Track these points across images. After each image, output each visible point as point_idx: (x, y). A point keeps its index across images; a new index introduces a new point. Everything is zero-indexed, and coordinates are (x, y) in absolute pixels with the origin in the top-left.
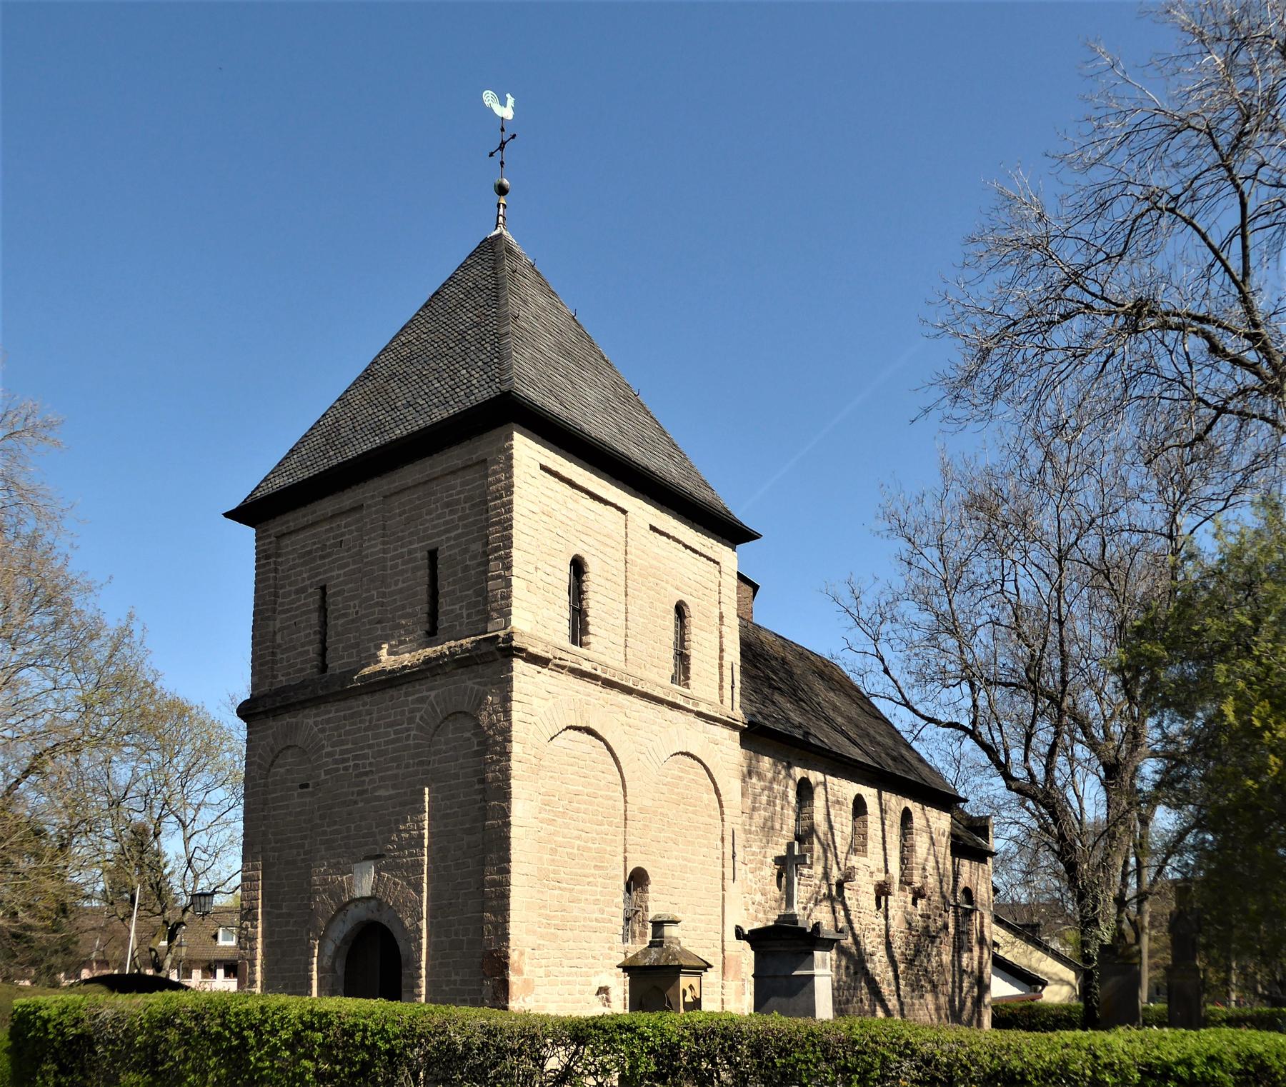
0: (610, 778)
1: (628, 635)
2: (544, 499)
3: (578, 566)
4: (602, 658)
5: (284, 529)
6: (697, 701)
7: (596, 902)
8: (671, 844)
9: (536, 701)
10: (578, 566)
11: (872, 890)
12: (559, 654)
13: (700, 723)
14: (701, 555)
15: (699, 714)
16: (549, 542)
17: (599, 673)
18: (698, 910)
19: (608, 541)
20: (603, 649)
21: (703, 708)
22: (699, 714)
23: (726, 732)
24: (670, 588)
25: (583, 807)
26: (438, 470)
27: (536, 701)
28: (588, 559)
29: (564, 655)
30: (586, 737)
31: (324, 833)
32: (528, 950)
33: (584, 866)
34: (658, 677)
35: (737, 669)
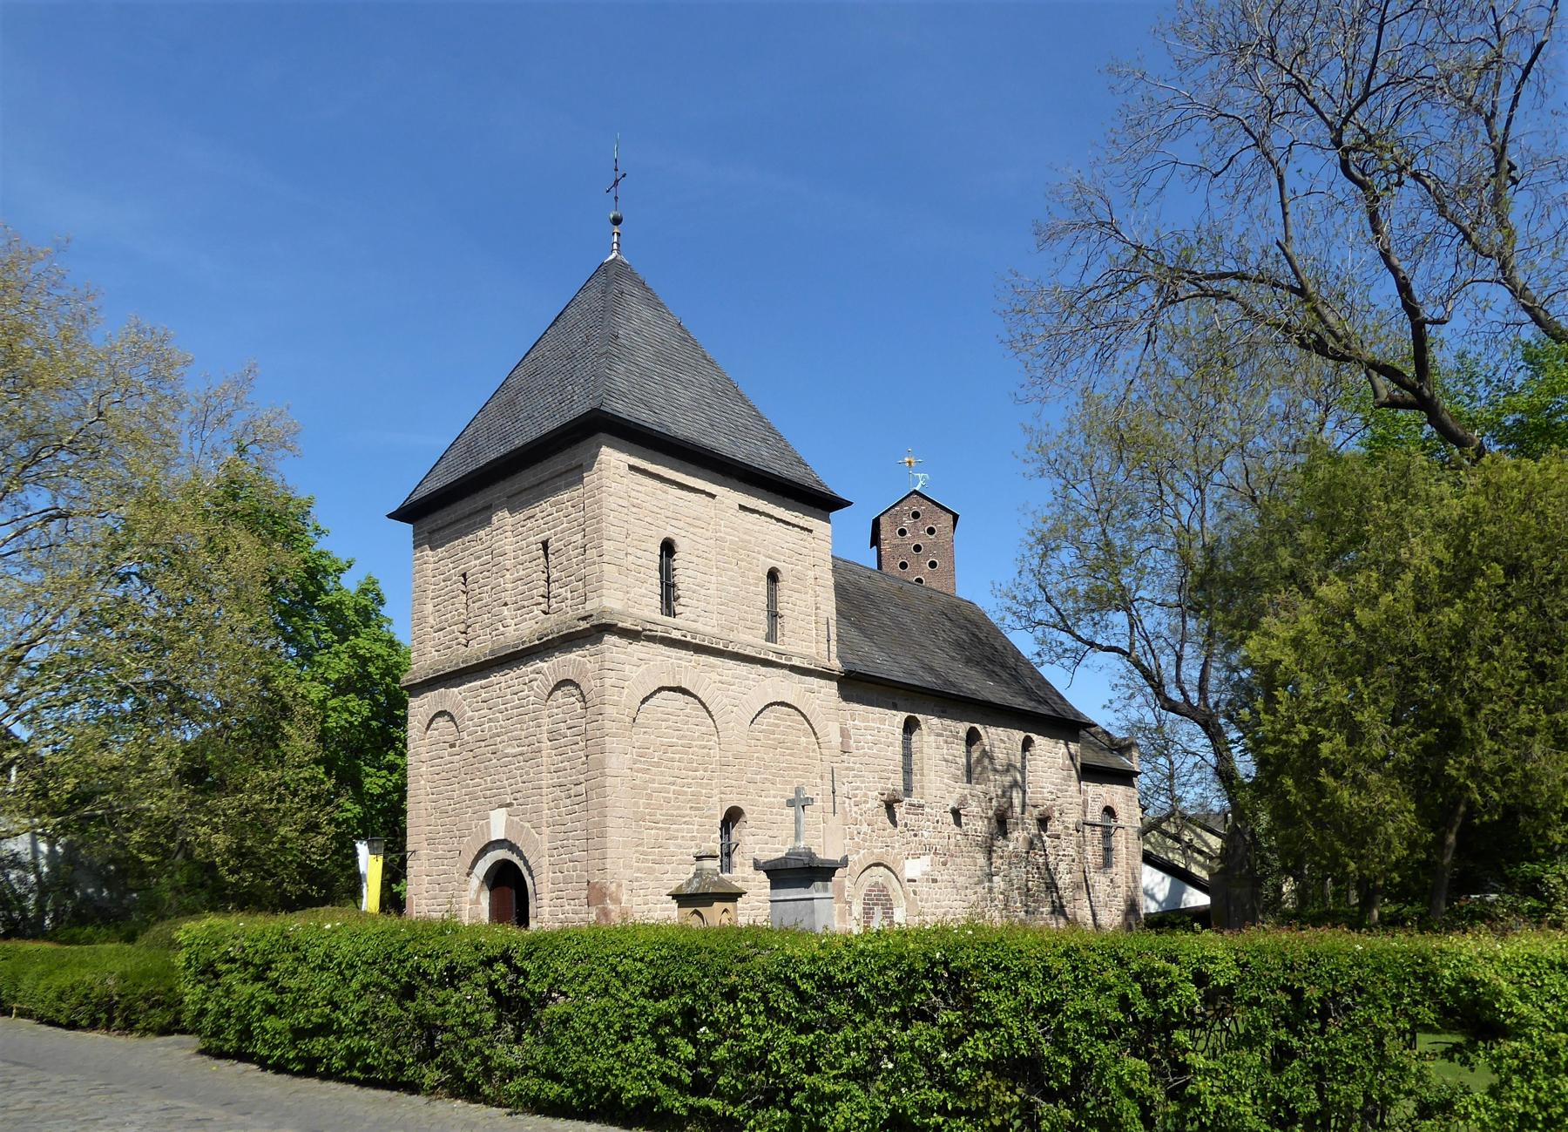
1: (716, 601)
2: (633, 494)
3: (668, 548)
4: (694, 626)
6: (790, 656)
7: (693, 839)
8: (768, 785)
9: (627, 667)
10: (668, 548)
12: (649, 626)
15: (793, 669)
16: (637, 529)
17: (689, 639)
21: (796, 662)
22: (793, 669)
23: (823, 682)
27: (627, 667)
28: (678, 540)
31: (468, 786)
32: (625, 882)
33: (679, 808)
35: (833, 623)
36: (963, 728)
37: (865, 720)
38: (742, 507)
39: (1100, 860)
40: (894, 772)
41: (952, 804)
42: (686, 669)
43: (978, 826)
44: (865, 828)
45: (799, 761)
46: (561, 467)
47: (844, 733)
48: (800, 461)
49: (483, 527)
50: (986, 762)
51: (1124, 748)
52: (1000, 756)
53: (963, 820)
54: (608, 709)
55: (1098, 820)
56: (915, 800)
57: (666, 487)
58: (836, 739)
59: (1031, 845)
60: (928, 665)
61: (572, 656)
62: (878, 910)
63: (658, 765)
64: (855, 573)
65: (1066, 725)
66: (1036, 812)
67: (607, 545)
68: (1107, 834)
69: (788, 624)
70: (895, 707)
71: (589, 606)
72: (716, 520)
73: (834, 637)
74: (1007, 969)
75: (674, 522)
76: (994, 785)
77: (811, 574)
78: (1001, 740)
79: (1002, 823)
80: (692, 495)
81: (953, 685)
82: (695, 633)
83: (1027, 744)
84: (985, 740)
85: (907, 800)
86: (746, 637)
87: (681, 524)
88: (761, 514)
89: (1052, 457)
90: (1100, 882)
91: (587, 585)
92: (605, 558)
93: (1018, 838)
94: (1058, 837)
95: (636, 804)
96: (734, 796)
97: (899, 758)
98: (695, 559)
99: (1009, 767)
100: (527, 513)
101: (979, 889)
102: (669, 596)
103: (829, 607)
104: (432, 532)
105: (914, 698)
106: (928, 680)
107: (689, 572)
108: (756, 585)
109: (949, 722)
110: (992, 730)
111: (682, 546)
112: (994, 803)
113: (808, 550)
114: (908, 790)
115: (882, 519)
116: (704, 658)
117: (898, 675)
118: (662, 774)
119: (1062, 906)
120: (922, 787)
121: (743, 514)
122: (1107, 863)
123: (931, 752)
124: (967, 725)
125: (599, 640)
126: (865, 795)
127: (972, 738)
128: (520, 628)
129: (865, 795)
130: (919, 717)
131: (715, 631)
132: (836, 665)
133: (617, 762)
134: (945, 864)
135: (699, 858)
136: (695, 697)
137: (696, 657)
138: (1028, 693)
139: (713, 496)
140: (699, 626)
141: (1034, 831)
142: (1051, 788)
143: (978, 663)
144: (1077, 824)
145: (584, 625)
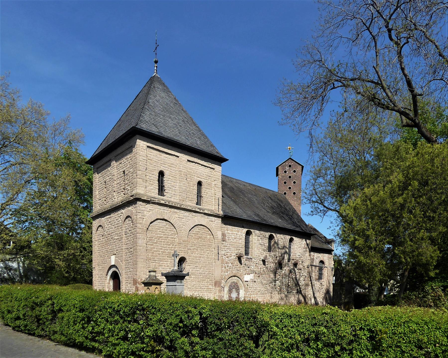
3: (161, 174)
4: (170, 199)
7: (168, 266)
9: (145, 212)
10: (161, 174)
14: (208, 167)
15: (205, 214)
16: (150, 167)
17: (167, 203)
18: (205, 268)
19: (172, 165)
21: (206, 212)
22: (205, 214)
23: (216, 218)
24: (196, 177)
25: (163, 241)
26: (124, 149)
27: (145, 212)
28: (165, 171)
29: (155, 199)
35: (220, 199)
36: (268, 234)
37: (232, 231)
38: (188, 161)
39: (317, 277)
40: (242, 248)
41: (262, 258)
43: (271, 265)
44: (230, 265)
45: (206, 243)
46: (127, 147)
47: (223, 235)
48: (212, 146)
49: (109, 167)
50: (276, 245)
51: (330, 242)
52: (281, 243)
53: (266, 263)
54: (139, 225)
55: (317, 265)
56: (249, 257)
57: (161, 153)
58: (220, 237)
59: (290, 272)
60: (259, 214)
61: (130, 208)
64: (239, 183)
65: (306, 233)
66: (293, 262)
67: (138, 172)
68: (321, 269)
69: (204, 200)
70: (243, 227)
71: (134, 192)
72: (179, 165)
73: (221, 204)
74: (155, 308)
75: (163, 165)
76: (278, 253)
77: (214, 183)
78: (282, 239)
79: (280, 265)
80: (170, 156)
81: (265, 220)
83: (291, 240)
84: (276, 238)
85: (245, 257)
86: (189, 203)
87: (166, 166)
88: (196, 163)
89: (320, 146)
90: (317, 284)
91: (134, 185)
92: (138, 177)
93: (286, 270)
94: (301, 269)
95: (148, 255)
97: (244, 243)
98: (171, 177)
99: (284, 247)
100: (120, 162)
101: (271, 285)
102: (161, 190)
103: (219, 194)
104: (97, 168)
105: (249, 224)
106: (256, 219)
107: (169, 182)
108: (193, 187)
109: (263, 232)
110: (278, 235)
111: (166, 173)
112: (278, 258)
113: (212, 176)
114: (247, 253)
116: (173, 210)
117: (245, 217)
118: (157, 246)
119: (301, 291)
120: (252, 253)
121: (189, 163)
122: (320, 277)
123: (255, 242)
124: (269, 233)
125: (136, 203)
126: (231, 254)
127: (271, 238)
128: (118, 199)
129: (231, 254)
130: (252, 230)
131: (178, 201)
132: (221, 213)
133: (141, 242)
134: (259, 277)
135: (150, 272)
136: (170, 222)
137: (170, 209)
138: (294, 224)
139: (178, 157)
141: (292, 267)
142: (299, 254)
143: (277, 214)
144: (308, 266)
145: (132, 198)
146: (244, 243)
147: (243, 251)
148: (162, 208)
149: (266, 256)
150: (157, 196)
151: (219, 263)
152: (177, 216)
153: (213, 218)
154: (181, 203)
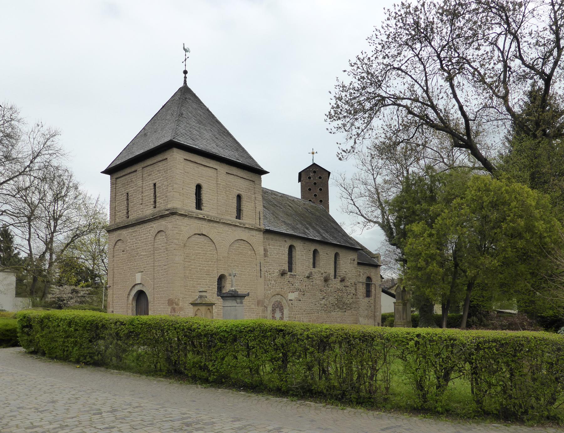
0: (211, 248)
4: (208, 213)
5: (117, 176)
9: (182, 227)
11: (322, 278)
13: (246, 230)
17: (206, 217)
20: (208, 209)
21: (247, 226)
23: (257, 233)
27: (182, 227)
30: (201, 237)
34: (231, 217)
40: (285, 263)
42: (205, 228)
44: (273, 282)
47: (265, 250)
56: (292, 273)
58: (262, 252)
62: (278, 310)
63: (194, 260)
71: (169, 206)
82: (208, 216)
85: (289, 273)
86: (228, 217)
96: (223, 271)
107: (207, 195)
108: (233, 200)
114: (290, 269)
115: (302, 173)
116: (211, 224)
134: (304, 295)
140: (211, 214)
145: (167, 212)
146: (287, 259)
147: (287, 268)
148: (200, 222)
149: (311, 273)
150: (194, 210)
151: (261, 280)
152: (216, 230)
153: (254, 233)
154: (220, 216)
